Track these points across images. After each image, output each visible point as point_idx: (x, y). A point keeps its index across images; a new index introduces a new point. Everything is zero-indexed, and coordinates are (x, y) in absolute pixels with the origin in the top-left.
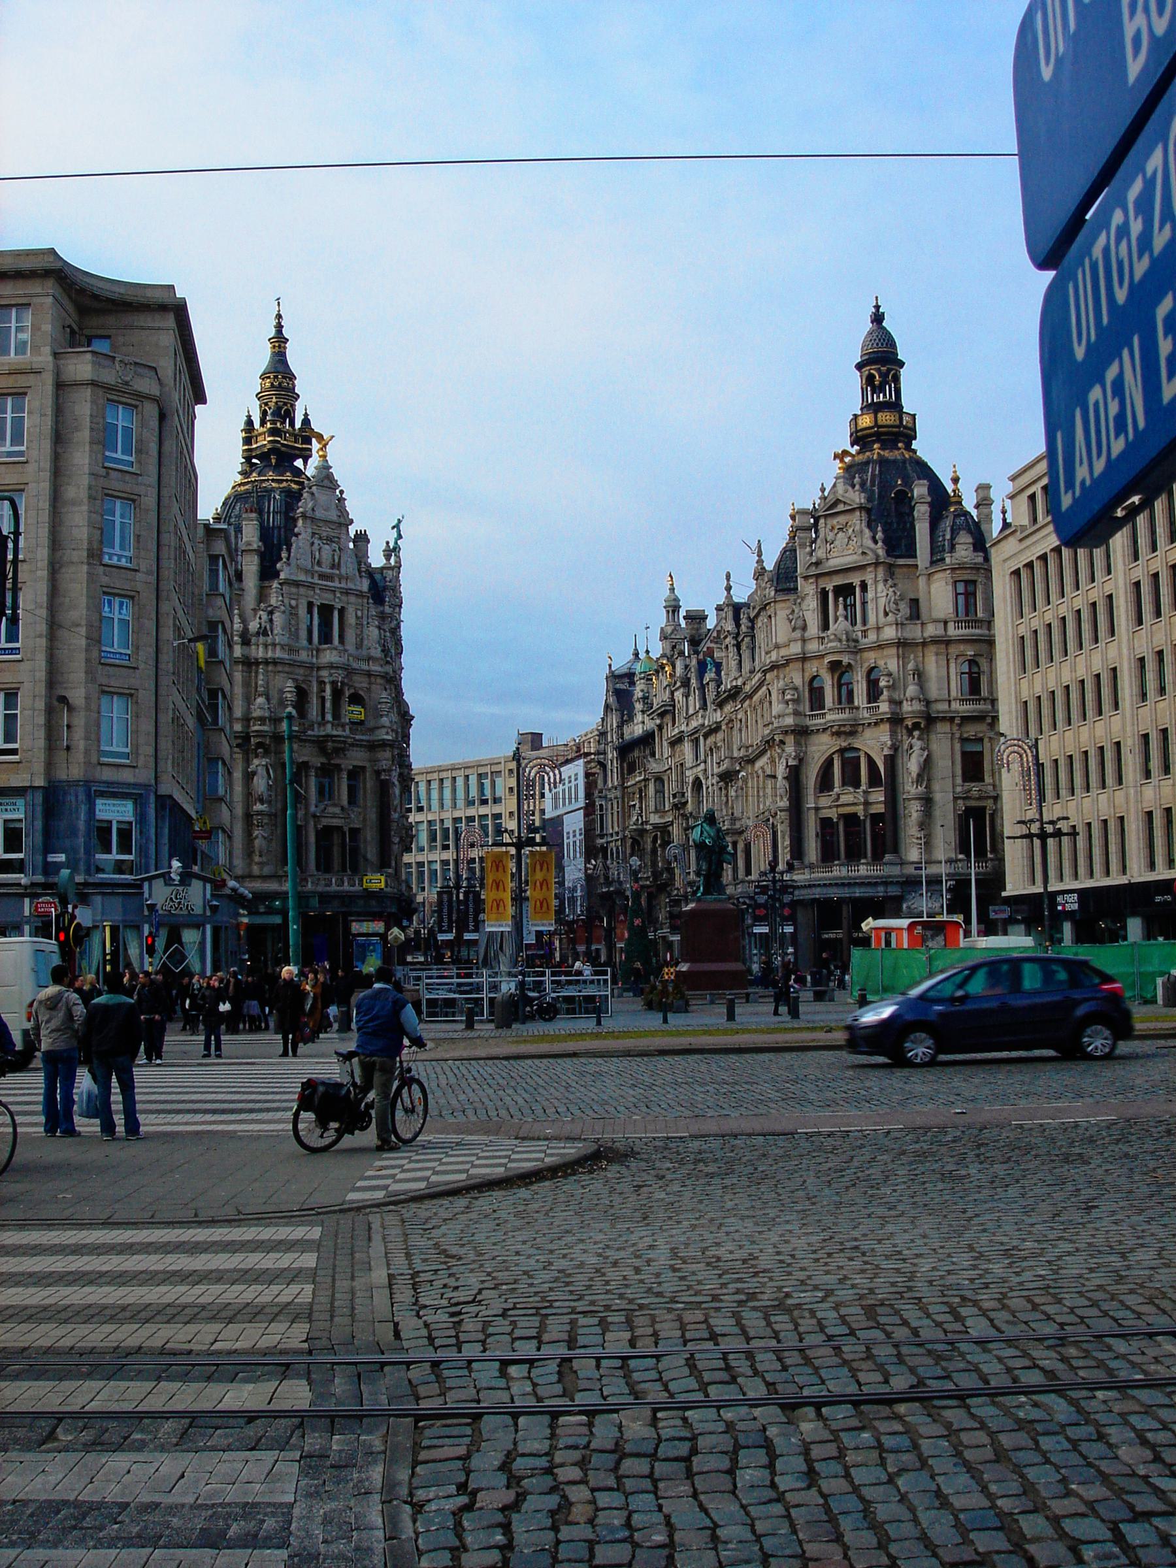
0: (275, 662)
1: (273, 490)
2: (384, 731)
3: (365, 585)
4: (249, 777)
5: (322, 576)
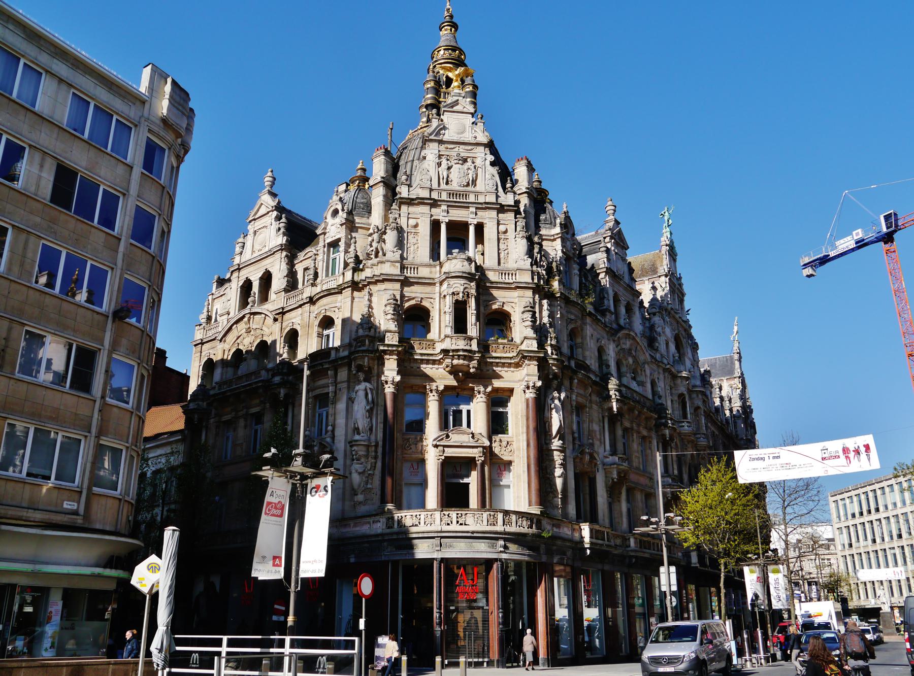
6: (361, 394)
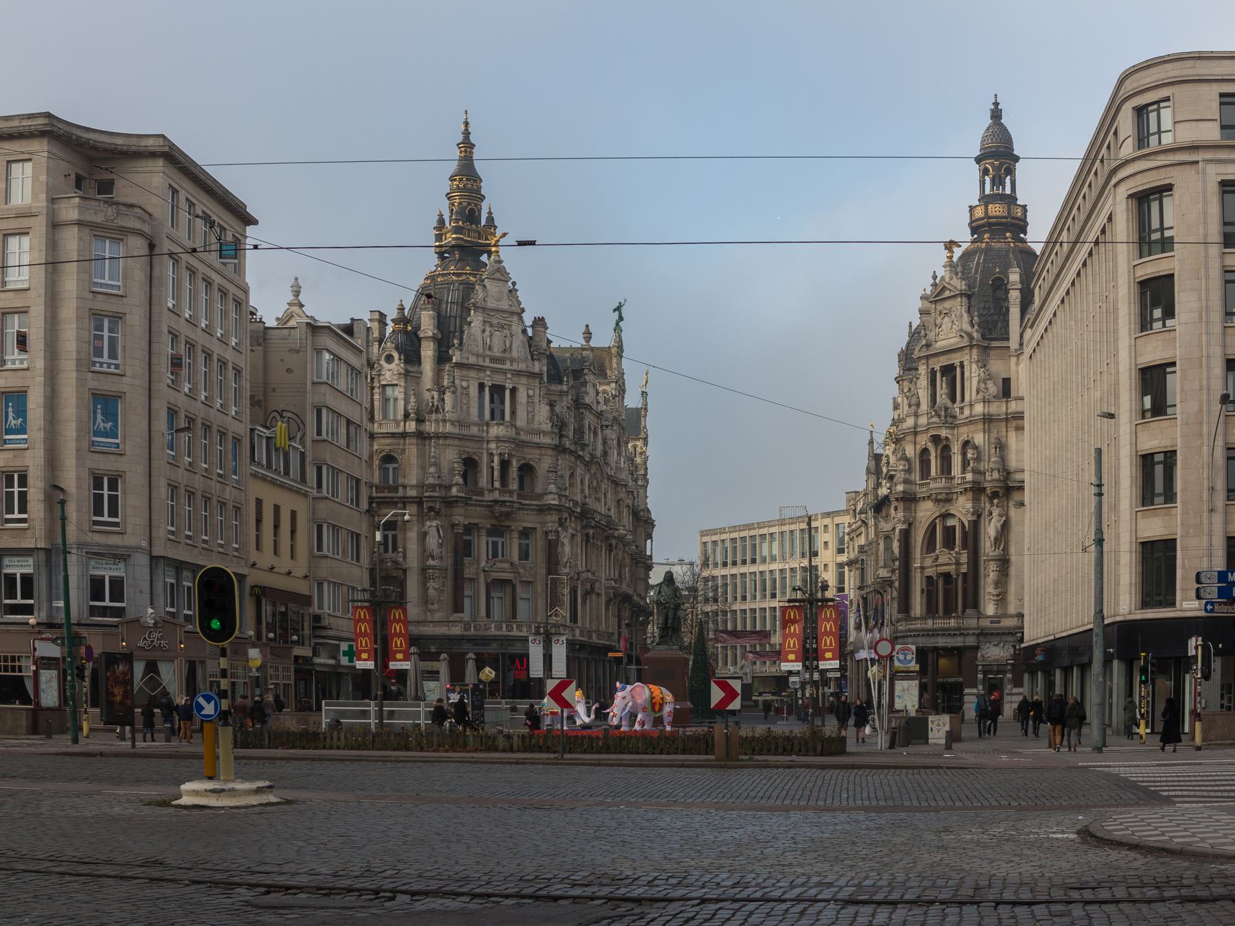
0: (446, 436)
1: (453, 283)
2: (551, 496)
3: (539, 366)
4: (423, 536)
5: (493, 360)
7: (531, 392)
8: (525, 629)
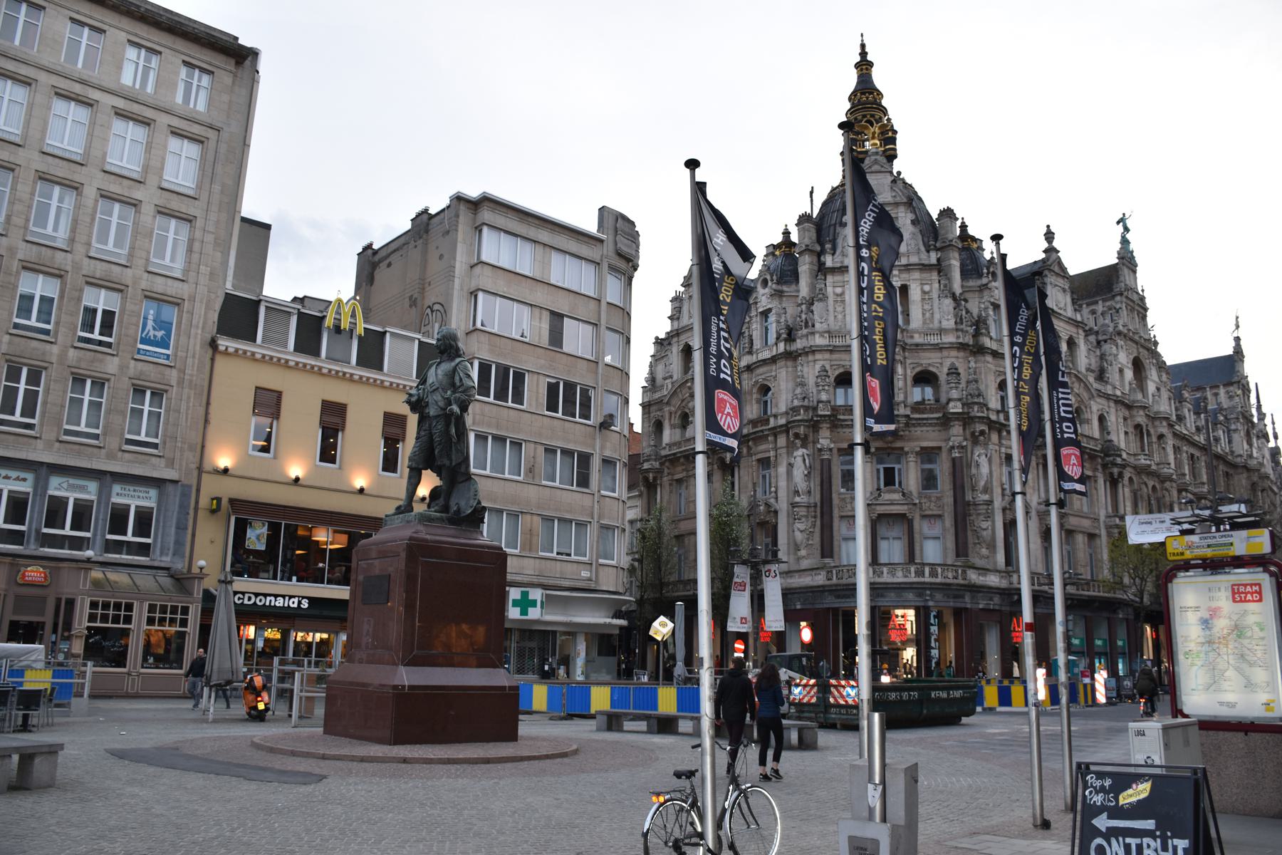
6: (799, 460)
7: (927, 288)
8: (900, 574)
